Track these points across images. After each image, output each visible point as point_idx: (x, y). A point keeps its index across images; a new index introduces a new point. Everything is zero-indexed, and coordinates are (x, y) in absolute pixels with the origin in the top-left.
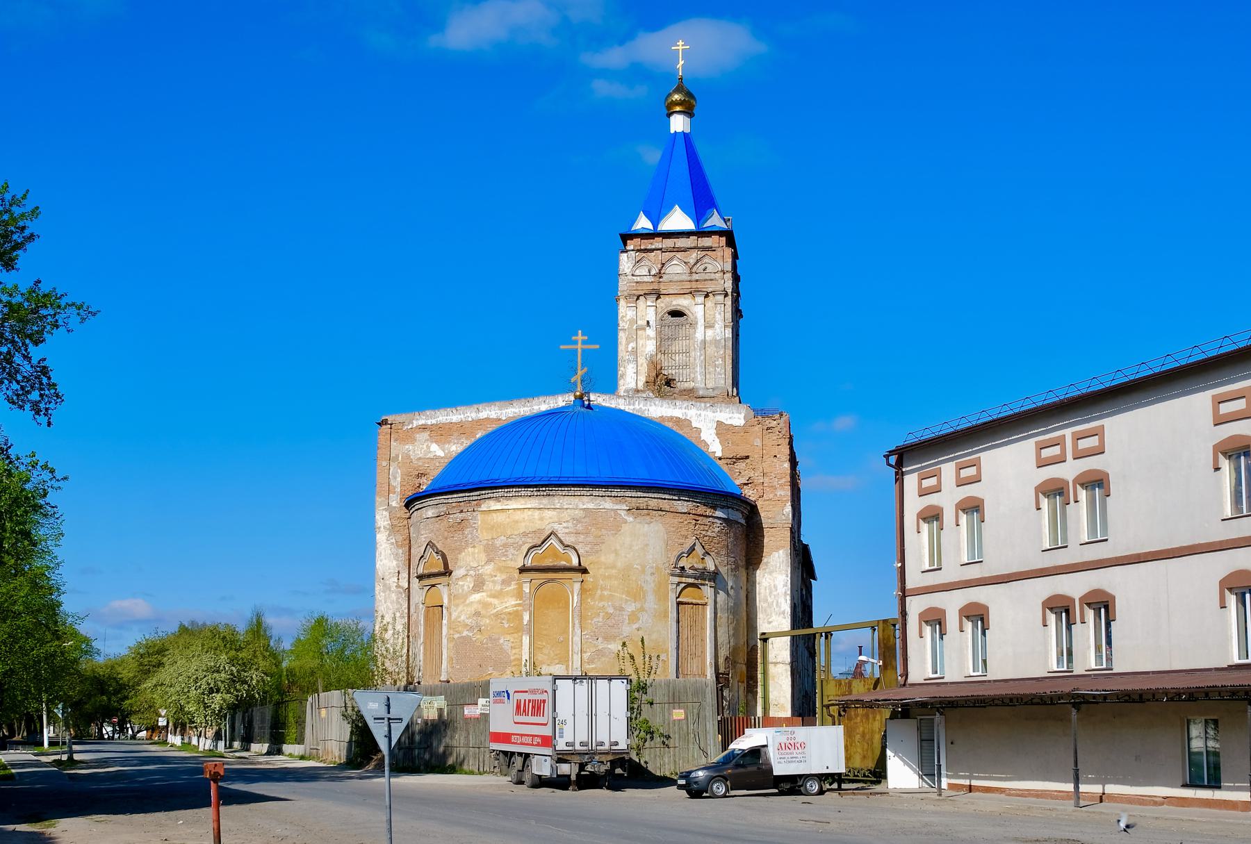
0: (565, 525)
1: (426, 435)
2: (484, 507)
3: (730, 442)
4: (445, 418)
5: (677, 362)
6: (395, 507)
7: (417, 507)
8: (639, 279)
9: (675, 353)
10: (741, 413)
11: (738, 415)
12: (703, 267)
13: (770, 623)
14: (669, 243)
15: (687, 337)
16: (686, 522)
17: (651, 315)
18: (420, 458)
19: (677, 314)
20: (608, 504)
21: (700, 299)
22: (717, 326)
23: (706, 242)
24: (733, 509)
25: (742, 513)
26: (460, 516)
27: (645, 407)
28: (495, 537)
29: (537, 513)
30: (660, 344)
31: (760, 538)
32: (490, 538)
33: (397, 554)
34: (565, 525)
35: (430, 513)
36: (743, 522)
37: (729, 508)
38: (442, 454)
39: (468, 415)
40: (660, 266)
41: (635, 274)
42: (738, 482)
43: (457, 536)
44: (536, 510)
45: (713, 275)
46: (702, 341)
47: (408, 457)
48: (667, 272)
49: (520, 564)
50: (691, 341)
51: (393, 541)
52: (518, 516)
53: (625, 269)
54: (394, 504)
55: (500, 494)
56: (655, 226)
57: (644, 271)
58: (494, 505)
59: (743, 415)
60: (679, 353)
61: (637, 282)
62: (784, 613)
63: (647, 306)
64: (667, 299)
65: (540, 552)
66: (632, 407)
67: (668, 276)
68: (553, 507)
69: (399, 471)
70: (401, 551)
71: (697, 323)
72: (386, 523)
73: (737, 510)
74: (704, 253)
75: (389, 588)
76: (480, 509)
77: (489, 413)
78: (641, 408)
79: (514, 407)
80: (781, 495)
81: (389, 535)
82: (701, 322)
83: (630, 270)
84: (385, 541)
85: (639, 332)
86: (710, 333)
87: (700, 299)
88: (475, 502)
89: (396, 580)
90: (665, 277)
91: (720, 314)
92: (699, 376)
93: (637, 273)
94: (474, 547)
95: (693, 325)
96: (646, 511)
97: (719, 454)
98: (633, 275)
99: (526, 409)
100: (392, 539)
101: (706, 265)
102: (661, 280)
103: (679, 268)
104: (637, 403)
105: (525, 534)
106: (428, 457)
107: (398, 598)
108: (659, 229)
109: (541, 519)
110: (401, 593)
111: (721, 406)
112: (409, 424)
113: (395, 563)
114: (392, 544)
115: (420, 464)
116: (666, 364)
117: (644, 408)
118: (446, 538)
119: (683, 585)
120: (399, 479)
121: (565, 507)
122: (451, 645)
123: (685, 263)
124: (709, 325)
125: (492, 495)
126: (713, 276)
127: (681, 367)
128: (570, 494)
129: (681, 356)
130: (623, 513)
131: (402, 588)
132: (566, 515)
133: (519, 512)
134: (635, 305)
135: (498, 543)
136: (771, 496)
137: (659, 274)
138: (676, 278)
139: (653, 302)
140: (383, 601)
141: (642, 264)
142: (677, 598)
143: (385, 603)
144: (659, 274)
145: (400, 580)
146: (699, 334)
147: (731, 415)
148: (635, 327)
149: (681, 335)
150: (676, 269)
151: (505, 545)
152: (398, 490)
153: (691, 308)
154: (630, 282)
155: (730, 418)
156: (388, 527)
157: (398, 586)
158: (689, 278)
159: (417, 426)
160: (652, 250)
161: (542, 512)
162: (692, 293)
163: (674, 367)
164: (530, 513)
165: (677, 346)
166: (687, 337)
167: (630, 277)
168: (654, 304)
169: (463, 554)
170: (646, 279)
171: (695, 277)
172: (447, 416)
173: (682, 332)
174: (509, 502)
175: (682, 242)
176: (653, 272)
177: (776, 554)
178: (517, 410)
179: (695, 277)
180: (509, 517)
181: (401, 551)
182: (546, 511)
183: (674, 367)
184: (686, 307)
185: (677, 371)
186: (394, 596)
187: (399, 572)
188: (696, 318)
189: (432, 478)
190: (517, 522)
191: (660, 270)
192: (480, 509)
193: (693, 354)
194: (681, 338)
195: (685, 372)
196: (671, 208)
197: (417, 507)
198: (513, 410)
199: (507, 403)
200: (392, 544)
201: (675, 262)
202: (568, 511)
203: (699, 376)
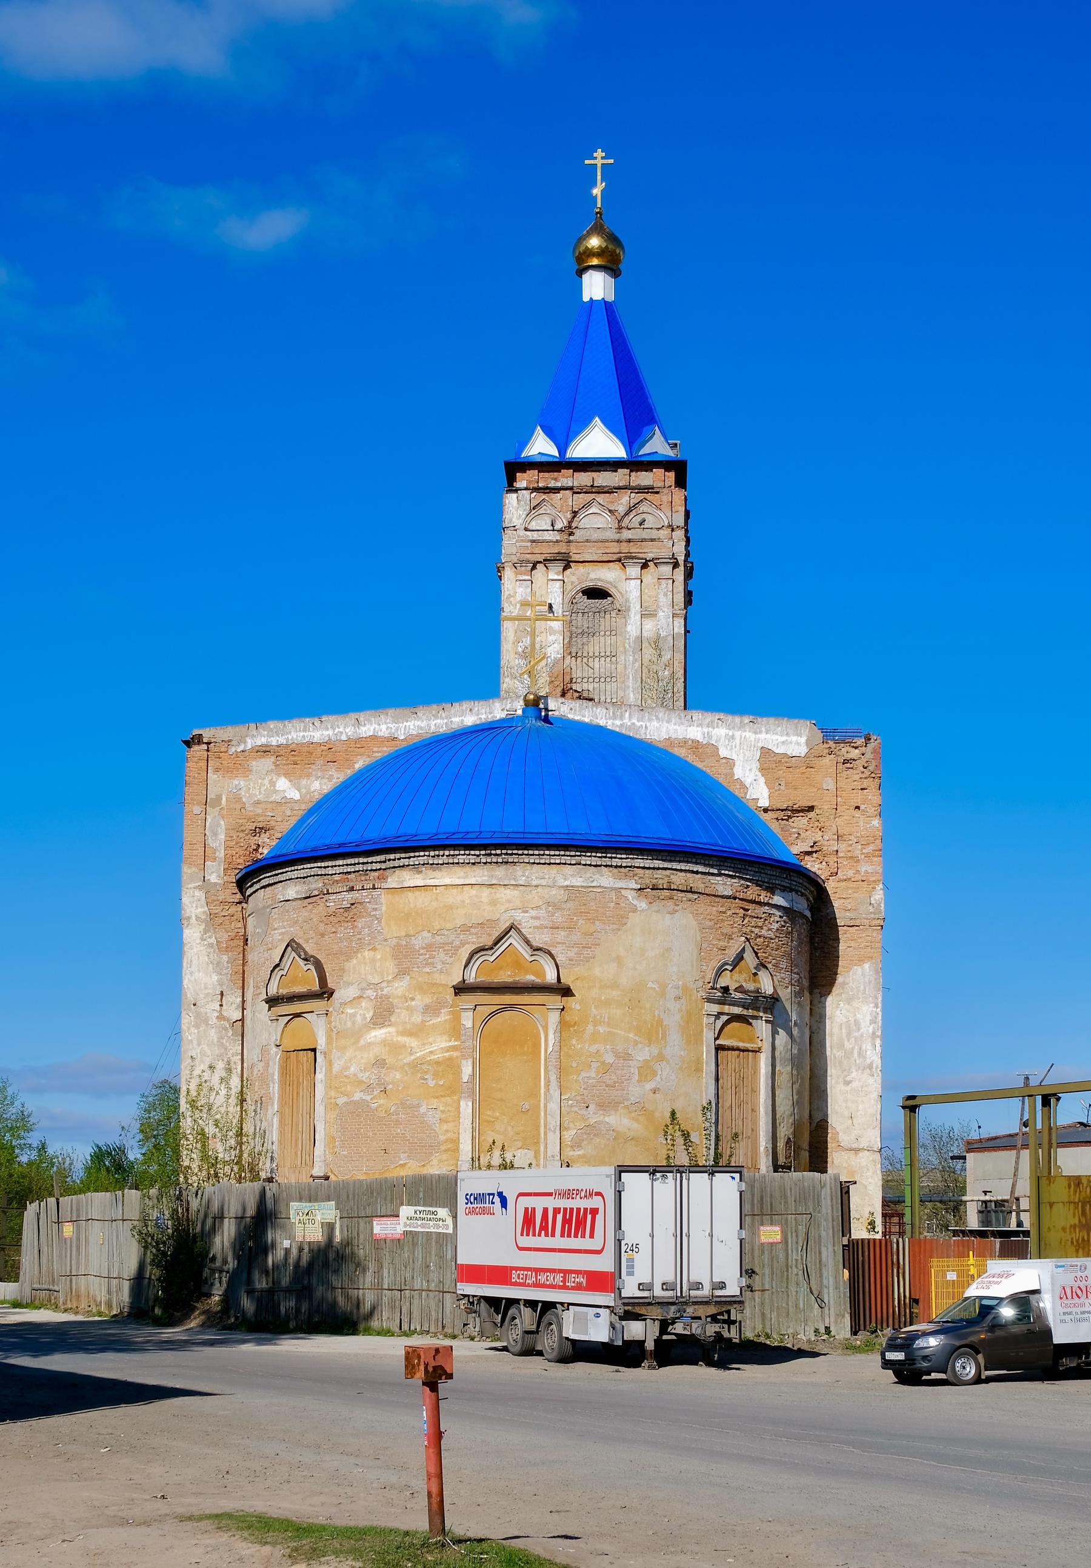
0: (533, 913)
1: (268, 762)
2: (393, 880)
3: (783, 783)
4: (302, 734)
5: (596, 670)
6: (215, 884)
7: (264, 883)
8: (535, 536)
9: (594, 657)
10: (800, 735)
11: (794, 739)
12: (639, 519)
13: (847, 1083)
14: (583, 479)
15: (613, 632)
16: (729, 913)
17: (555, 595)
18: (258, 802)
19: (596, 593)
20: (605, 879)
21: (634, 570)
22: (661, 614)
23: (644, 478)
24: (797, 892)
25: (808, 899)
26: (350, 897)
27: (641, 723)
28: (412, 933)
29: (486, 893)
30: (570, 642)
31: (831, 943)
32: (403, 934)
33: (218, 963)
34: (533, 913)
35: (292, 891)
36: (808, 914)
37: (791, 890)
39: (341, 730)
40: (569, 516)
41: (530, 527)
42: (795, 850)
43: (344, 931)
44: (485, 889)
45: (655, 532)
46: (637, 638)
47: (239, 799)
48: (581, 525)
49: (456, 979)
50: (619, 638)
51: (213, 940)
52: (453, 897)
53: (514, 520)
54: (213, 878)
55: (421, 860)
56: (562, 450)
57: (544, 523)
58: (409, 878)
59: (803, 740)
60: (600, 657)
61: (533, 541)
62: (870, 1067)
63: (548, 580)
65: (492, 959)
66: (618, 722)
67: (582, 532)
68: (513, 882)
69: (222, 823)
70: (225, 958)
71: (629, 610)
72: (200, 910)
73: (802, 895)
74: (641, 496)
78: (634, 724)
79: (419, 719)
80: (866, 872)
81: (205, 931)
82: (635, 608)
83: (521, 521)
84: (199, 941)
86: (649, 625)
87: (634, 570)
88: (376, 874)
89: (218, 1007)
90: (578, 535)
91: (666, 595)
92: (632, 695)
93: (533, 525)
94: (374, 949)
96: (667, 893)
97: (764, 803)
98: (526, 529)
101: (644, 516)
102: (571, 538)
103: (600, 518)
104: (627, 714)
105: (465, 929)
106: (270, 800)
109: (494, 903)
110: (226, 1029)
111: (768, 723)
113: (215, 978)
114: (211, 945)
115: (259, 811)
116: (579, 674)
117: (638, 724)
118: (323, 935)
119: (725, 1018)
120: (222, 837)
121: (534, 883)
122: (333, 1115)
123: (610, 511)
124: (647, 614)
125: (406, 861)
126: (654, 534)
127: (602, 680)
128: (542, 861)
129: (602, 662)
130: (631, 895)
131: (228, 1020)
132: (534, 897)
133: (454, 891)
134: (529, 578)
135: (417, 943)
136: (850, 873)
137: (569, 530)
138: (596, 536)
139: (557, 574)
140: (195, 1042)
141: (541, 511)
142: (716, 1039)
143: (199, 1045)
144: (569, 530)
145: (224, 1007)
146: (633, 626)
147: (784, 738)
149: (602, 628)
151: (429, 947)
152: (221, 854)
154: (522, 541)
155: (783, 742)
156: (203, 917)
157: (221, 1017)
158: (617, 537)
160: (556, 490)
161: (494, 891)
162: (621, 561)
163: (591, 680)
164: (473, 892)
165: (595, 646)
166: (613, 632)
167: (522, 533)
168: (560, 577)
169: (355, 961)
171: (626, 534)
172: (304, 731)
173: (605, 623)
174: (437, 874)
175: (604, 479)
176: (559, 525)
177: (858, 970)
178: (423, 724)
179: (626, 534)
180: (437, 899)
181: (225, 958)
182: (502, 889)
183: (591, 680)
184: (611, 583)
185: (596, 685)
186: (213, 1034)
187: (222, 994)
188: (627, 601)
189: (280, 835)
190: (450, 907)
191: (570, 522)
193: (621, 658)
194: (602, 633)
195: (608, 687)
196: (586, 422)
197: (264, 883)
199: (407, 711)
200: (211, 945)
201: (593, 510)
202: (539, 889)
203: (632, 695)
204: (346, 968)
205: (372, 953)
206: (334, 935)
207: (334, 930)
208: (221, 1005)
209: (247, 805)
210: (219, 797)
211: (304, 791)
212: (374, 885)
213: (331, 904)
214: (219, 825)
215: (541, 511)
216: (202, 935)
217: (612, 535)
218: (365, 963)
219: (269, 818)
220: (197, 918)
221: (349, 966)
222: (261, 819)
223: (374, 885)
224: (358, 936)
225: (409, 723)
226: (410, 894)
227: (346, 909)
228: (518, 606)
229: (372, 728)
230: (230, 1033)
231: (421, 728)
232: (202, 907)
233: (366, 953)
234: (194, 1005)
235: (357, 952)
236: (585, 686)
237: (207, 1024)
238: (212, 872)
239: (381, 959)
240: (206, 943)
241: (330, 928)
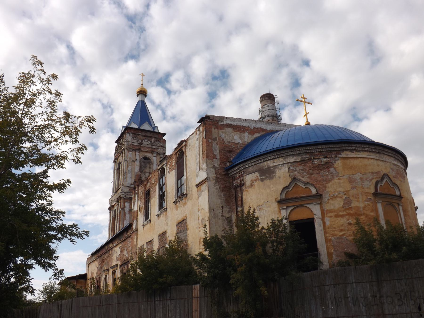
2: (343, 155)
8: (133, 144)
9: (146, 173)
14: (144, 134)
15: (150, 168)
17: (138, 157)
18: (229, 142)
19: (146, 158)
21: (155, 155)
23: (157, 136)
26: (325, 160)
28: (354, 173)
29: (375, 162)
32: (351, 174)
33: (220, 195)
38: (241, 142)
39: (251, 124)
45: (160, 147)
47: (223, 140)
48: (144, 143)
50: (151, 169)
51: (218, 187)
52: (366, 162)
54: (216, 165)
55: (353, 148)
57: (135, 141)
61: (133, 145)
64: (143, 153)
67: (144, 145)
70: (222, 194)
72: (213, 175)
75: (218, 217)
76: (340, 156)
77: (261, 125)
81: (215, 183)
84: (213, 186)
85: (133, 163)
87: (155, 155)
88: (335, 152)
89: (221, 212)
90: (143, 145)
93: (133, 141)
94: (339, 179)
95: (152, 163)
98: (131, 142)
99: (278, 127)
100: (217, 186)
105: (372, 173)
106: (233, 141)
107: (223, 224)
108: (141, 128)
110: (224, 220)
112: (221, 122)
113: (219, 201)
115: (230, 145)
116: (142, 176)
131: (225, 217)
133: (366, 160)
137: (141, 144)
138: (147, 146)
139: (138, 153)
140: (214, 224)
141: (135, 139)
145: (223, 212)
148: (131, 161)
150: (146, 143)
151: (361, 179)
152: (218, 157)
153: (152, 158)
157: (222, 216)
158: (151, 147)
159: (226, 124)
162: (152, 153)
164: (372, 161)
165: (147, 170)
166: (150, 168)
167: (130, 142)
170: (136, 144)
171: (154, 147)
172: (241, 122)
173: (148, 166)
174: (359, 153)
176: (139, 142)
178: (274, 127)
179: (154, 147)
180: (361, 162)
181: (222, 194)
186: (220, 222)
187: (222, 207)
189: (236, 154)
190: (366, 166)
191: (141, 142)
192: (340, 156)
198: (272, 127)
200: (217, 189)
204: (327, 186)
205: (338, 181)
206: (318, 174)
207: (318, 172)
208: (222, 211)
209: (226, 142)
210: (216, 138)
211: (243, 141)
212: (336, 156)
213: (315, 163)
214: (217, 147)
215: (135, 139)
216: (214, 185)
217: (150, 146)
218: (336, 184)
219: (233, 148)
220: (212, 178)
221: (328, 185)
222: (230, 147)
223: (336, 156)
224: (331, 174)
225: (270, 126)
226: (351, 160)
227: (323, 164)
228: (129, 158)
229: (260, 125)
230: (226, 222)
231: (273, 128)
232: (214, 174)
233: (336, 180)
234: (213, 210)
235: (332, 180)
236: (144, 179)
237: (218, 218)
238: (216, 163)
239: (343, 183)
240: (216, 187)
241: (315, 172)
